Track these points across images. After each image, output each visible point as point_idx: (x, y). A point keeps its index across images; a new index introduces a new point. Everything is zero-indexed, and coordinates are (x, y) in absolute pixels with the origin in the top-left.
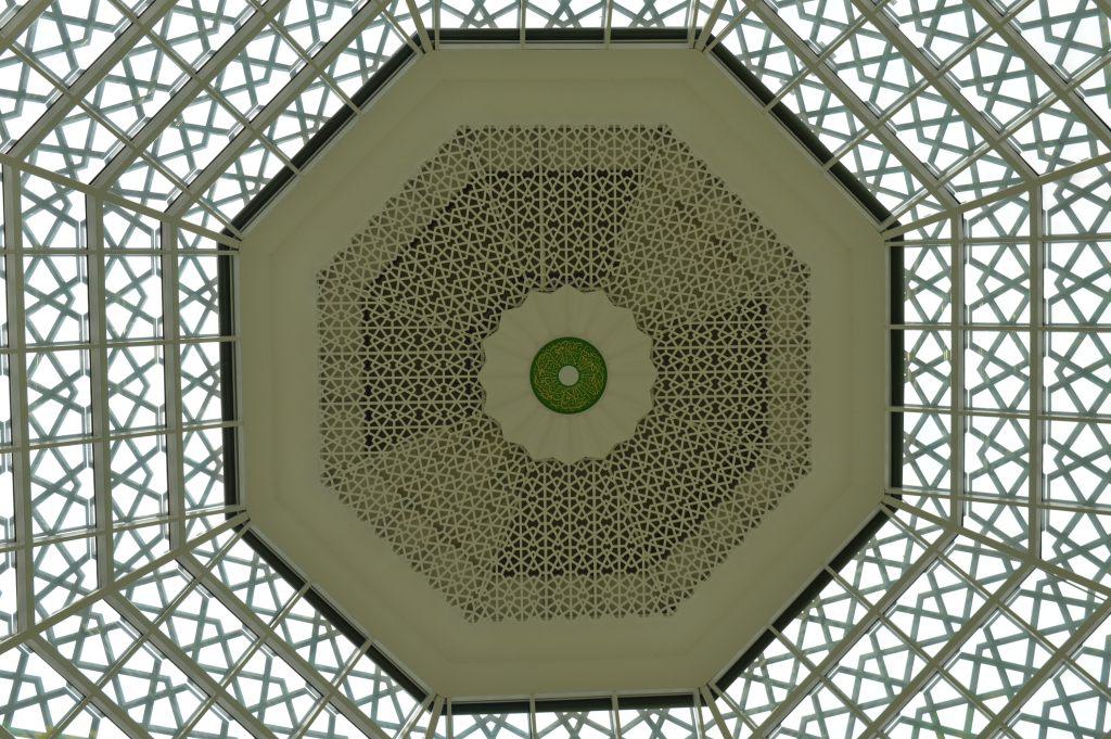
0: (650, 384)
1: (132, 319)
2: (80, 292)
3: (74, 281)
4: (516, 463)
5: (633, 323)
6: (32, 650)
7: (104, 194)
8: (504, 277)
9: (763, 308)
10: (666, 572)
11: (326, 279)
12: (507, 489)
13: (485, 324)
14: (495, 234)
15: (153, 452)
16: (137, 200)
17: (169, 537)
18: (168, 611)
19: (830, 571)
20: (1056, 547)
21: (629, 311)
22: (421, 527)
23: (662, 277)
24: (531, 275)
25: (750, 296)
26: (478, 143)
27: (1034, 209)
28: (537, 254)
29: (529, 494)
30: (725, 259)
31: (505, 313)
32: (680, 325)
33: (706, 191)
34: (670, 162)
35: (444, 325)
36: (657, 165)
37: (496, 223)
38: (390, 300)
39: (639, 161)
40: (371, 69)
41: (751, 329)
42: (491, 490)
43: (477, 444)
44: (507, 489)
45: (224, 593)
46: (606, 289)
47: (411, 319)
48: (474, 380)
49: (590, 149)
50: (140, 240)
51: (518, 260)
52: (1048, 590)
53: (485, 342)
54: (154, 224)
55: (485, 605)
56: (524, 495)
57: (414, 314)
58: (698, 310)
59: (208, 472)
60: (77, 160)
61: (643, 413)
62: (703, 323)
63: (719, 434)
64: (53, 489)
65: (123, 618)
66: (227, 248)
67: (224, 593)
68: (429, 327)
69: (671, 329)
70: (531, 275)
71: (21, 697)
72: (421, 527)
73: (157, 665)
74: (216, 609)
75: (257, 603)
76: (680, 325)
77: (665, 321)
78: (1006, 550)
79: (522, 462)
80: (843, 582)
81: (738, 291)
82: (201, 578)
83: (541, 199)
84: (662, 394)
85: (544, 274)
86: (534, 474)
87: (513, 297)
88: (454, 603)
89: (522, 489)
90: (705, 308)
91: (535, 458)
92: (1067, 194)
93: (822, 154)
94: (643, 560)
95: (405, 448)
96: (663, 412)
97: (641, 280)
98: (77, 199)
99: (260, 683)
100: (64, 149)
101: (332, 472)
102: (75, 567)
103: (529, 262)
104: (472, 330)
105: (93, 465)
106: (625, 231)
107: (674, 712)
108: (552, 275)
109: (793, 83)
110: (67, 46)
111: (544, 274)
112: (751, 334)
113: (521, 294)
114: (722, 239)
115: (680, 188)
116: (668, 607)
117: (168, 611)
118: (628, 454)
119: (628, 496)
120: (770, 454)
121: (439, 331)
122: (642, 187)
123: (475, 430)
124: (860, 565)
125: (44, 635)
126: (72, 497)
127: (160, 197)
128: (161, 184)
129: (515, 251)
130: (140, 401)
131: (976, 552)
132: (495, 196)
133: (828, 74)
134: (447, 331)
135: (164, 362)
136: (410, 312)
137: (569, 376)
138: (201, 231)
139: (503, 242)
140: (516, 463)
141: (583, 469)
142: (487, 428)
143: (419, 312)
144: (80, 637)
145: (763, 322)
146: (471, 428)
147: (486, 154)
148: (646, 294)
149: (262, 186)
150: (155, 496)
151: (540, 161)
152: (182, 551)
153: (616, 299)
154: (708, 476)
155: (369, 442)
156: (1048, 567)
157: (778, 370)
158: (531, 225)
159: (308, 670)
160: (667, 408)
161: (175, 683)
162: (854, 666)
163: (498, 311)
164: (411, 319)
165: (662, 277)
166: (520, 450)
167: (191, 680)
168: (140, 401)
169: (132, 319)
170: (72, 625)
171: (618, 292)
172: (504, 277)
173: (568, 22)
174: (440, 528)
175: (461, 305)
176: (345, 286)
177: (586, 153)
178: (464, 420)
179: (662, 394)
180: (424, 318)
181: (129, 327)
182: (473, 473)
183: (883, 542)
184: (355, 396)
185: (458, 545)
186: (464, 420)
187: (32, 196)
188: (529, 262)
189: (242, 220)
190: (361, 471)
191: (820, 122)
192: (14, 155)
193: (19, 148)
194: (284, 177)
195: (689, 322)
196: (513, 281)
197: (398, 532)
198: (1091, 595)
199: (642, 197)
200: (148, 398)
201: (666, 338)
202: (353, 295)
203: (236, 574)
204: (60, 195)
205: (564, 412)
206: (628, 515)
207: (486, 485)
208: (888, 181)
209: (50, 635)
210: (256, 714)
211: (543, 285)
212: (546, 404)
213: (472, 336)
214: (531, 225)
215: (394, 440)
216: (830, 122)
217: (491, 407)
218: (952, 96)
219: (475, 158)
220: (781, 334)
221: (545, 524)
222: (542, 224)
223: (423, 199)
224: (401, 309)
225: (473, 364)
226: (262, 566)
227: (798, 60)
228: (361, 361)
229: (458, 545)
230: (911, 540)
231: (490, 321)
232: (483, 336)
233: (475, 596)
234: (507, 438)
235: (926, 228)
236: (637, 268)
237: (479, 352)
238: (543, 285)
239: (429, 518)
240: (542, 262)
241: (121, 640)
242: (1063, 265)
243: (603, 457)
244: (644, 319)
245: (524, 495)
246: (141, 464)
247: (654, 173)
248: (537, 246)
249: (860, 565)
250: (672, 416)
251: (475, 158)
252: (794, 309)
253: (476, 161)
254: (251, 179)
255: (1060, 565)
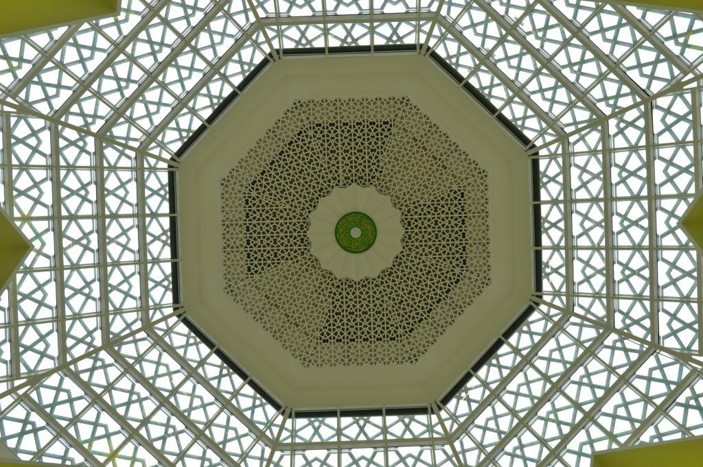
0: (401, 236)
1: (121, 204)
2: (92, 189)
3: (89, 183)
4: (329, 281)
5: (390, 204)
6: (66, 376)
7: (104, 138)
8: (321, 181)
9: (462, 194)
10: (412, 340)
11: (225, 183)
12: (324, 295)
13: (311, 205)
14: (315, 157)
15: (133, 274)
16: (123, 142)
17: (141, 320)
18: (140, 359)
19: (503, 339)
20: (623, 321)
21: (388, 197)
22: (277, 316)
23: (406, 178)
24: (335, 179)
25: (455, 188)
26: (305, 108)
27: (605, 137)
28: (338, 167)
29: (336, 297)
30: (440, 168)
31: (321, 199)
32: (417, 204)
33: (429, 131)
34: (409, 116)
35: (288, 207)
36: (402, 118)
37: (315, 151)
38: (259, 194)
39: (392, 116)
40: (247, 71)
41: (456, 206)
42: (315, 295)
43: (307, 270)
44: (324, 295)
45: (171, 350)
46: (376, 186)
47: (270, 204)
48: (305, 236)
49: (365, 110)
50: (125, 162)
51: (328, 171)
52: (619, 345)
53: (311, 215)
54: (132, 154)
55: (313, 358)
56: (333, 298)
57: (272, 201)
58: (426, 196)
59: (164, 286)
60: (90, 120)
61: (397, 252)
62: (429, 203)
63: (439, 264)
64: (77, 292)
65: (116, 361)
66: (172, 167)
67: (171, 350)
68: (280, 208)
69: (412, 207)
70: (335, 179)
71: (60, 399)
72: (277, 316)
73: (133, 386)
74: (166, 358)
75: (189, 356)
76: (417, 204)
77: (408, 202)
78: (597, 324)
79: (332, 280)
80: (510, 345)
81: (448, 185)
82: (158, 342)
83: (339, 138)
84: (407, 242)
85: (341, 178)
86: (338, 287)
87: (325, 191)
88: (296, 357)
89: (332, 295)
90: (430, 195)
91: (338, 278)
92: (622, 125)
93: (492, 109)
94: (399, 333)
95: (269, 273)
96: (408, 252)
97: (394, 180)
98: (90, 141)
99: (155, 366)
100: (82, 114)
101: (230, 286)
102: (90, 333)
103: (334, 172)
104: (303, 209)
105: (99, 280)
106: (385, 154)
107: (417, 417)
108: (346, 178)
109: (474, 71)
110: (82, 61)
111: (341, 178)
112: (456, 209)
113: (329, 189)
114: (439, 157)
115: (414, 130)
116: (413, 359)
117: (140, 359)
118: (389, 275)
119: (390, 298)
120: (468, 275)
121: (285, 210)
122: (394, 130)
123: (306, 263)
124: (520, 336)
125: (72, 367)
126: (88, 297)
127: (135, 140)
128: (135, 133)
129: (326, 166)
130: (125, 247)
131: (581, 326)
132: (315, 136)
133: (492, 66)
134: (290, 210)
135: (138, 227)
136: (270, 200)
137: (356, 233)
138: (159, 158)
139: (319, 161)
140: (329, 281)
141: (365, 282)
142: (312, 262)
143: (275, 199)
144: (92, 370)
145: (462, 202)
146: (303, 262)
147: (309, 114)
148: (397, 188)
149: (191, 134)
150: (134, 298)
151: (338, 118)
152: (148, 326)
153: (381, 191)
154: (434, 287)
155: (249, 270)
156: (619, 332)
157: (472, 229)
158: (334, 152)
159: (216, 392)
160: (410, 249)
161: (143, 396)
162: (514, 390)
163: (317, 198)
164: (270, 204)
165: (406, 178)
166: (330, 274)
167: (151, 394)
168: (125, 247)
169: (121, 204)
170: (86, 364)
171: (382, 187)
172: (321, 181)
173: (352, 43)
174: (288, 316)
175: (297, 196)
176: (235, 187)
177: (363, 112)
178: (300, 258)
179: (407, 242)
180: (277, 203)
181: (119, 209)
182: (305, 286)
183: (532, 322)
184: (242, 246)
185: (298, 326)
186: (300, 258)
187: (66, 139)
188: (334, 172)
189: (180, 153)
190: (245, 285)
191: (490, 92)
192: (55, 117)
193: (58, 113)
194: (202, 129)
195: (422, 202)
196: (325, 182)
197: (265, 318)
198: (642, 346)
199: (394, 135)
200: (130, 246)
201: (409, 211)
202: (240, 191)
203: (178, 341)
204: (81, 138)
205: (353, 252)
206: (390, 308)
207: (312, 293)
208: (529, 123)
209: (76, 367)
210: (221, 446)
211: (341, 183)
212: (344, 248)
213: (303, 212)
214: (334, 152)
215: (263, 269)
216: (495, 91)
217: (314, 250)
218: (556, 73)
219: (303, 116)
220: (473, 208)
221: (345, 313)
222: (340, 151)
223: (276, 139)
224: (265, 198)
225: (305, 226)
226: (193, 337)
227: (476, 60)
228: (244, 227)
229: (298, 326)
230: (547, 321)
231: (313, 204)
232: (309, 212)
233: (308, 353)
234: (323, 267)
235: (551, 147)
236: (392, 174)
237: (307, 221)
238: (341, 183)
239: (282, 311)
240: (340, 171)
241: (114, 372)
242: (621, 165)
243: (376, 277)
244: (397, 201)
245: (333, 298)
246: (125, 278)
247: (400, 122)
248: (338, 163)
249: (520, 336)
250: (413, 254)
251: (303, 116)
252: (479, 195)
253: (304, 118)
254: (184, 130)
255: (625, 331)
